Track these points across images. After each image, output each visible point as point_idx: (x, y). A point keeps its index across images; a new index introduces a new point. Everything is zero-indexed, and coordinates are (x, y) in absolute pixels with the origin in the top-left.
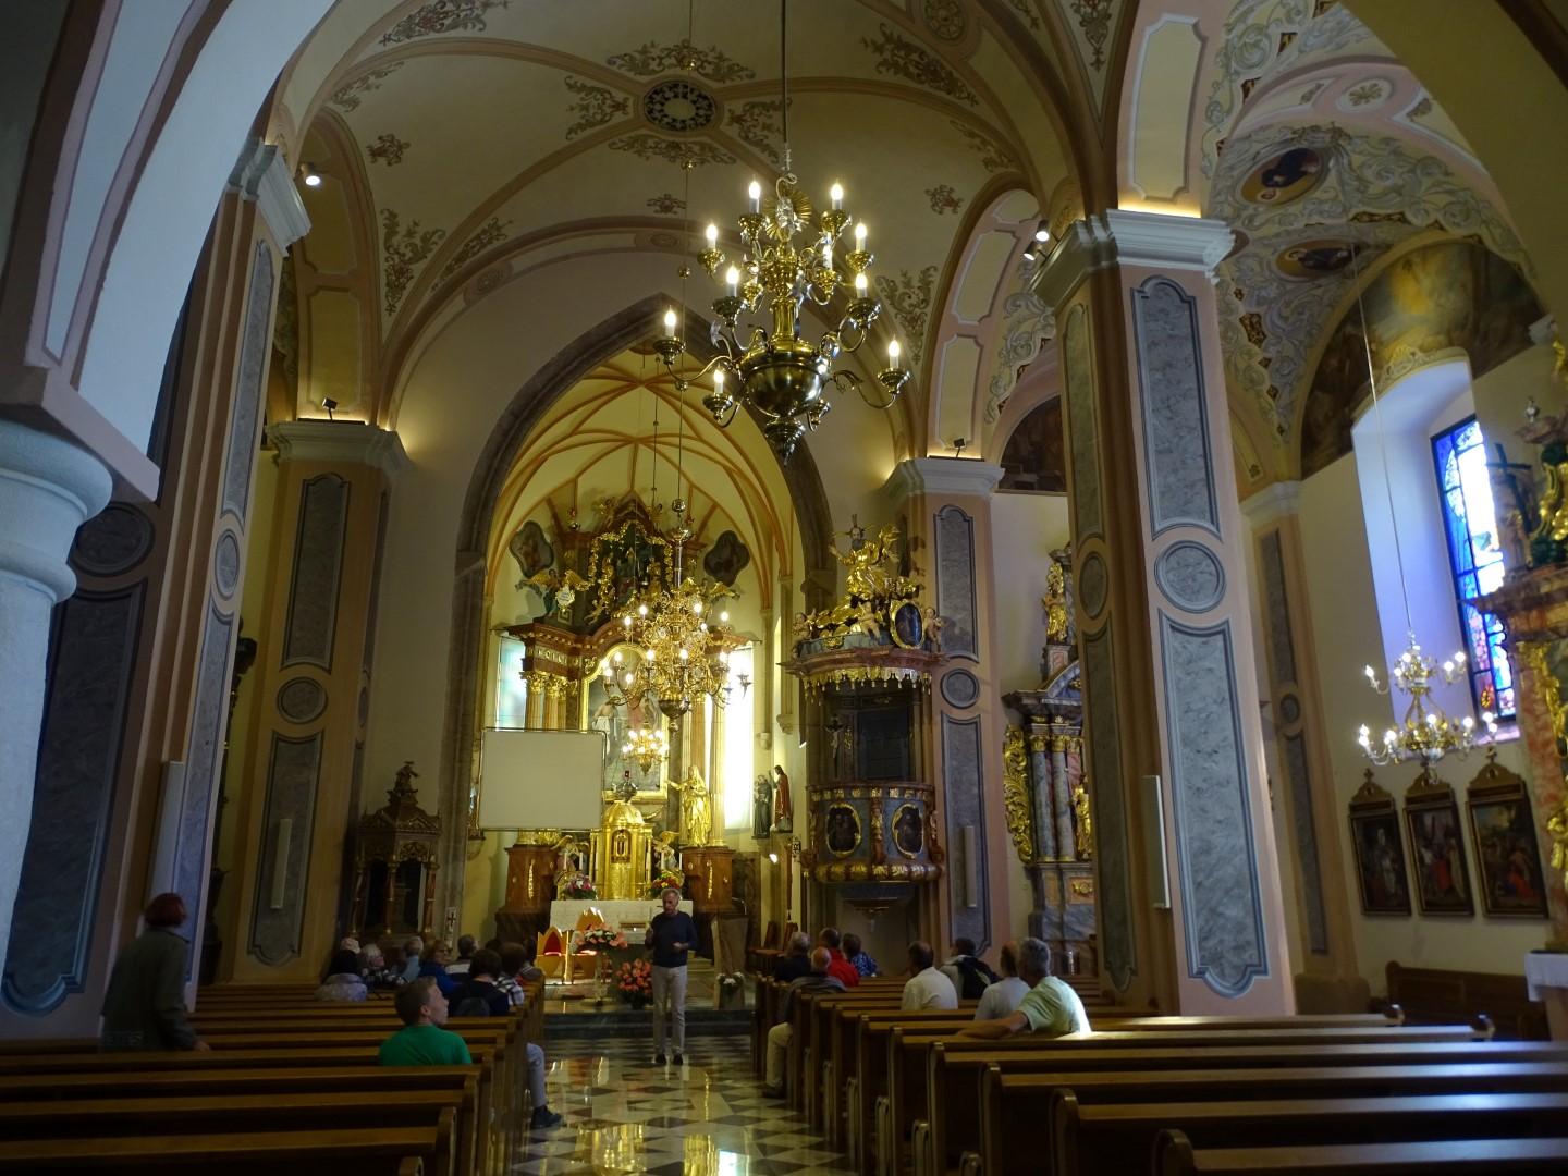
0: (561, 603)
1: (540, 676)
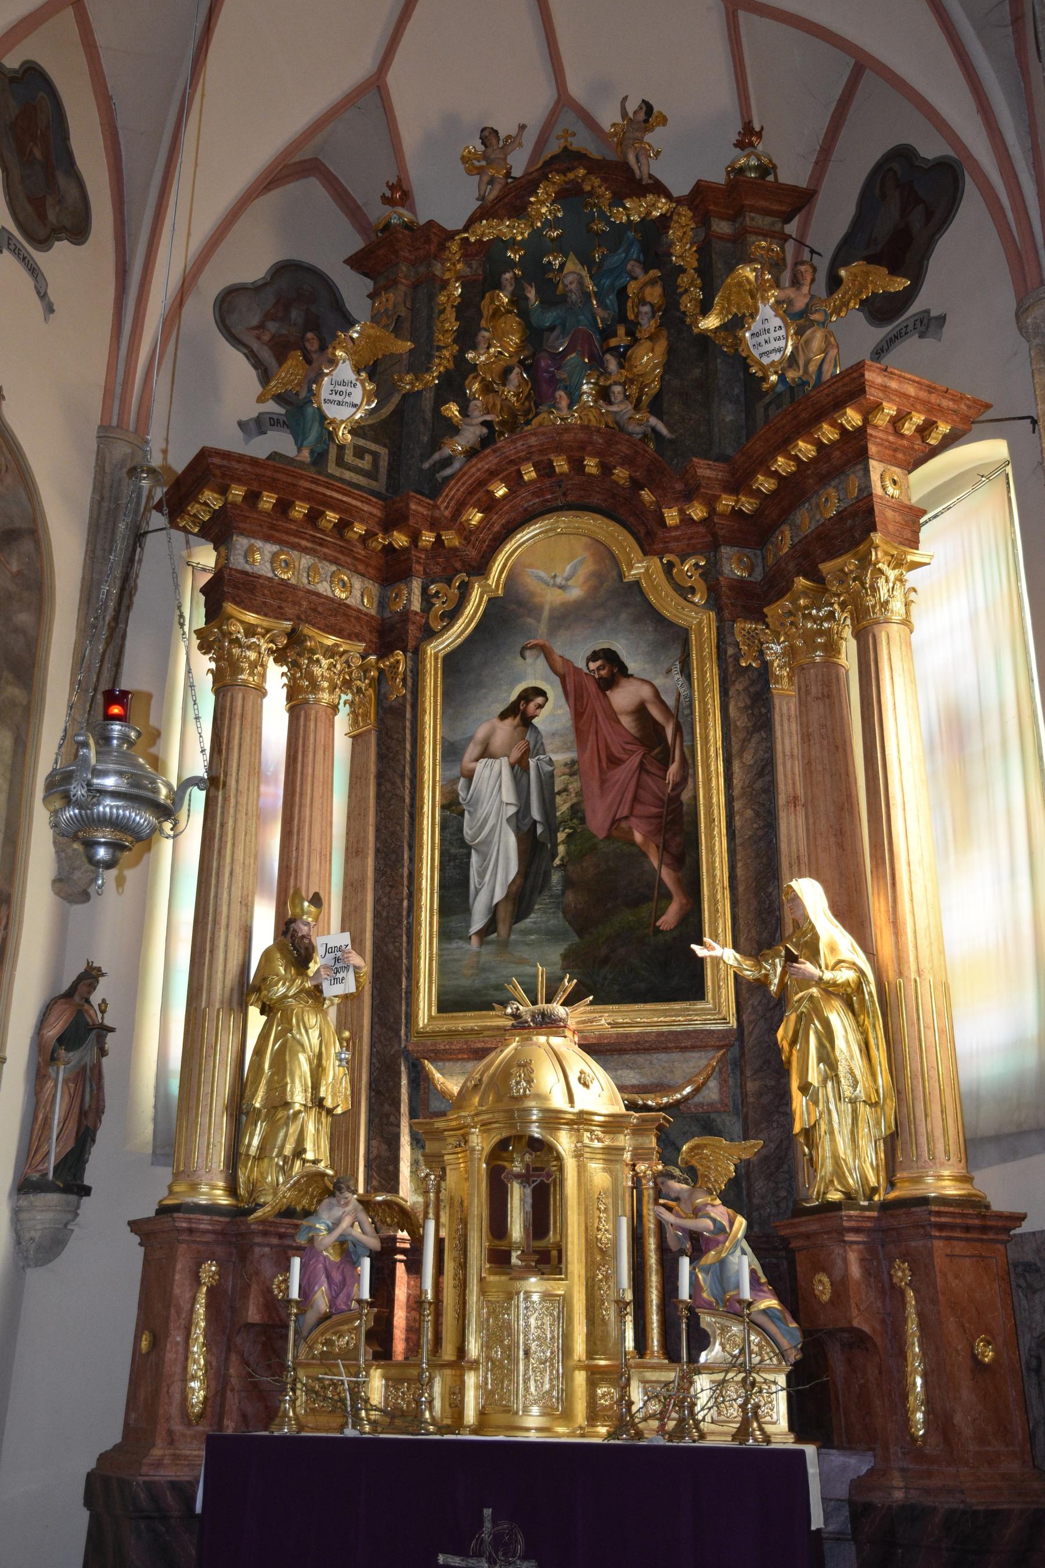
0: (331, 412)
1: (250, 630)
